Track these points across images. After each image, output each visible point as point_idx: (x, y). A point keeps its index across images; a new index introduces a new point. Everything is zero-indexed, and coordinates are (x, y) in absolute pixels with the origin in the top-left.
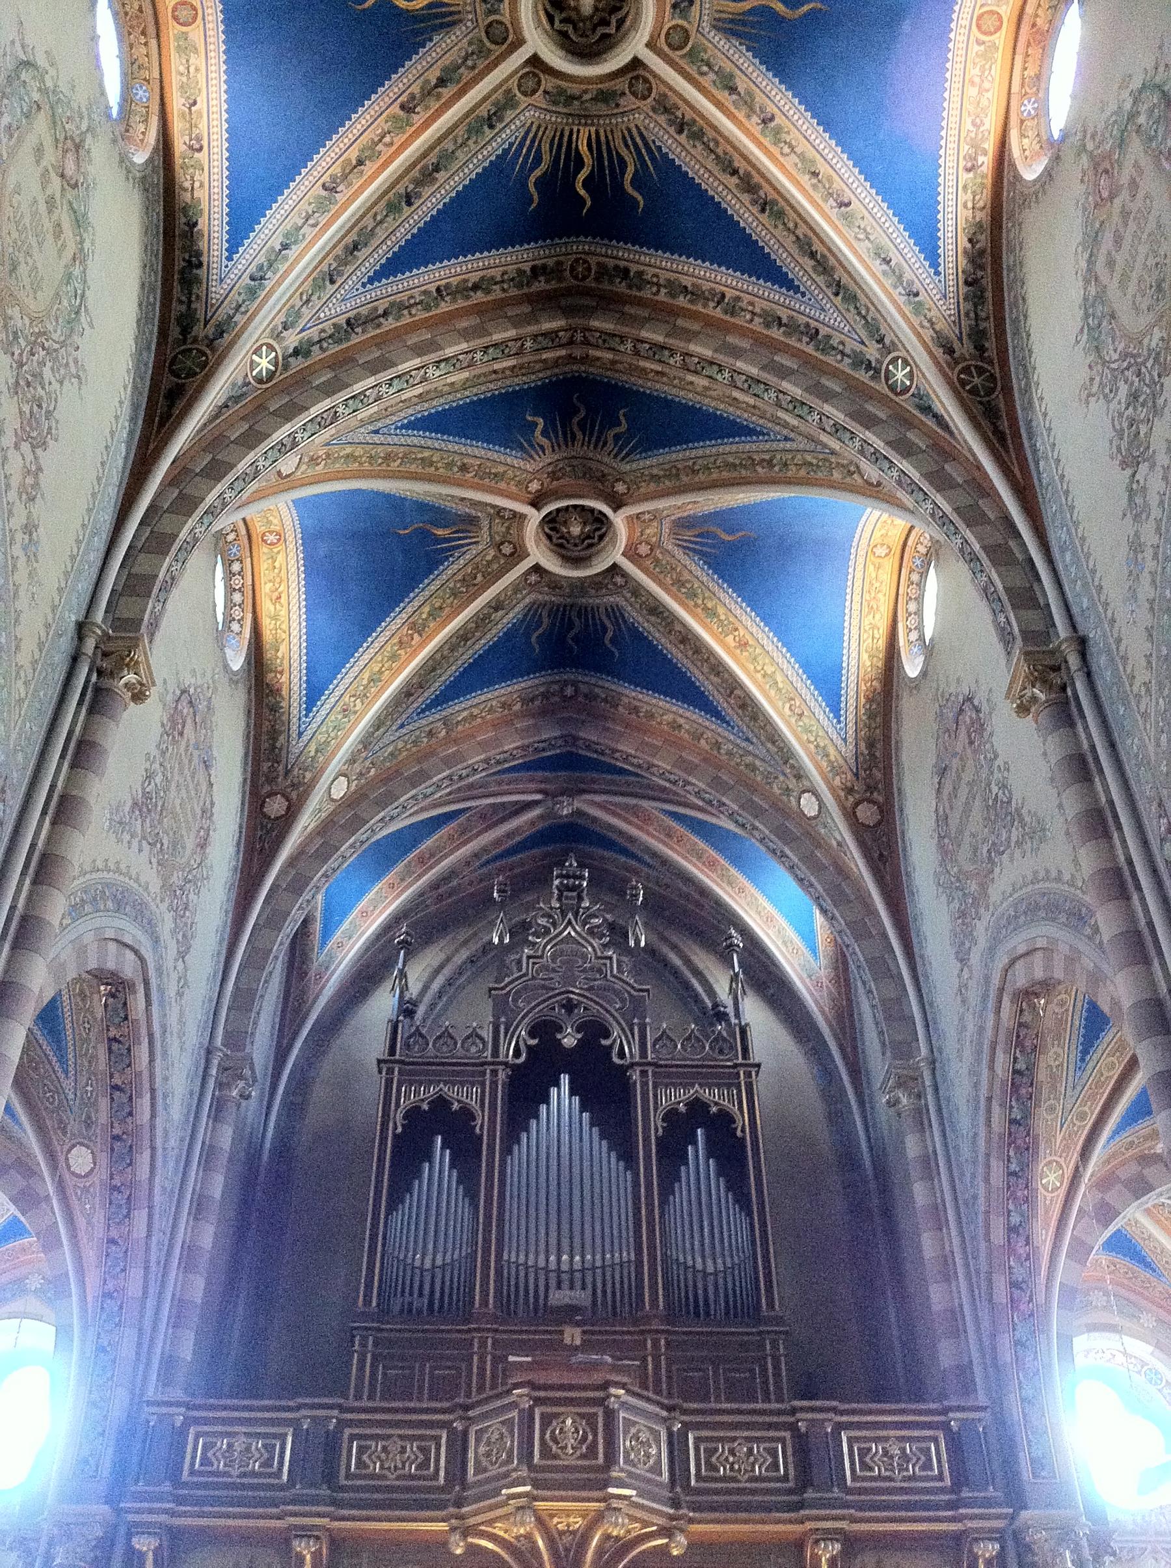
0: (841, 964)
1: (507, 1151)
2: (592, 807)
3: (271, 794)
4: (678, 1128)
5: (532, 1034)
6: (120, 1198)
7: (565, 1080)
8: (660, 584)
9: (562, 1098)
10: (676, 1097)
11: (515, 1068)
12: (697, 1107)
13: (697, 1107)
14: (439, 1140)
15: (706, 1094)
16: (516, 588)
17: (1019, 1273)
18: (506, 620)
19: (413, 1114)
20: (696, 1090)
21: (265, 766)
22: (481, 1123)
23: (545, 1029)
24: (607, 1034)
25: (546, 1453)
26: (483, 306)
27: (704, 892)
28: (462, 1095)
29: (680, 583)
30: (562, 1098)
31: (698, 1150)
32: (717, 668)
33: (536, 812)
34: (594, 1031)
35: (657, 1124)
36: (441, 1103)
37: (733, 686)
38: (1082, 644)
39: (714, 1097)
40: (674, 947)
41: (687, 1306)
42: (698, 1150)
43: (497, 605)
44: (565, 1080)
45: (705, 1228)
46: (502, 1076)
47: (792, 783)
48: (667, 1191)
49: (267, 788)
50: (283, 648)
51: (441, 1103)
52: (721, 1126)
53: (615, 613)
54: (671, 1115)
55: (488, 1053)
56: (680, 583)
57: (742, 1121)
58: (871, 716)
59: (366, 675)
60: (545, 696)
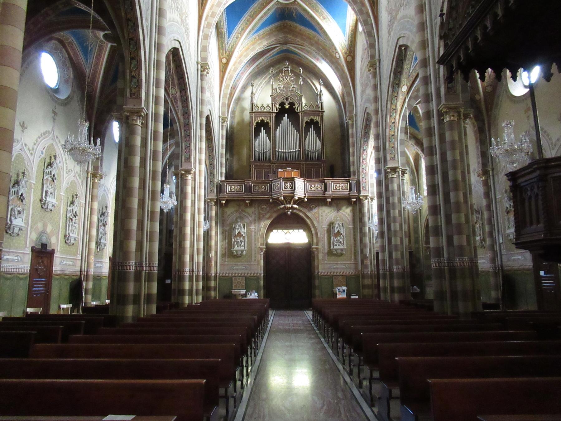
0: (343, 93)
1: (276, 130)
2: (290, 47)
3: (223, 58)
4: (308, 124)
5: (280, 105)
6: (211, 149)
7: (286, 115)
8: (305, 4)
9: (286, 118)
10: (308, 119)
11: (276, 113)
12: (312, 120)
13: (312, 120)
14: (262, 128)
15: (313, 118)
16: (273, 6)
17: (364, 157)
18: (271, 13)
19: (257, 123)
20: (312, 117)
21: (221, 51)
22: (270, 125)
23: (282, 104)
24: (294, 105)
25: (285, 188)
26: (270, 34)
27: (316, 66)
28: (266, 119)
29: (310, 4)
30: (286, 118)
31: (312, 130)
32: (318, 24)
33: (278, 48)
34: (292, 104)
35: (304, 124)
36: (262, 121)
37: (322, 28)
38: (380, 61)
39: (316, 119)
40: (309, 78)
41: (309, 159)
42: (312, 130)
43: (269, 10)
44: (286, 115)
45: (313, 142)
46: (274, 115)
47: (334, 50)
48: (306, 137)
49: (222, 57)
50: (222, 23)
51: (262, 121)
52: (316, 124)
53: (296, 9)
54: (307, 123)
55: (271, 110)
56: (310, 4)
57: (320, 123)
58: (352, 35)
59: (241, 29)
60: (280, 26)
